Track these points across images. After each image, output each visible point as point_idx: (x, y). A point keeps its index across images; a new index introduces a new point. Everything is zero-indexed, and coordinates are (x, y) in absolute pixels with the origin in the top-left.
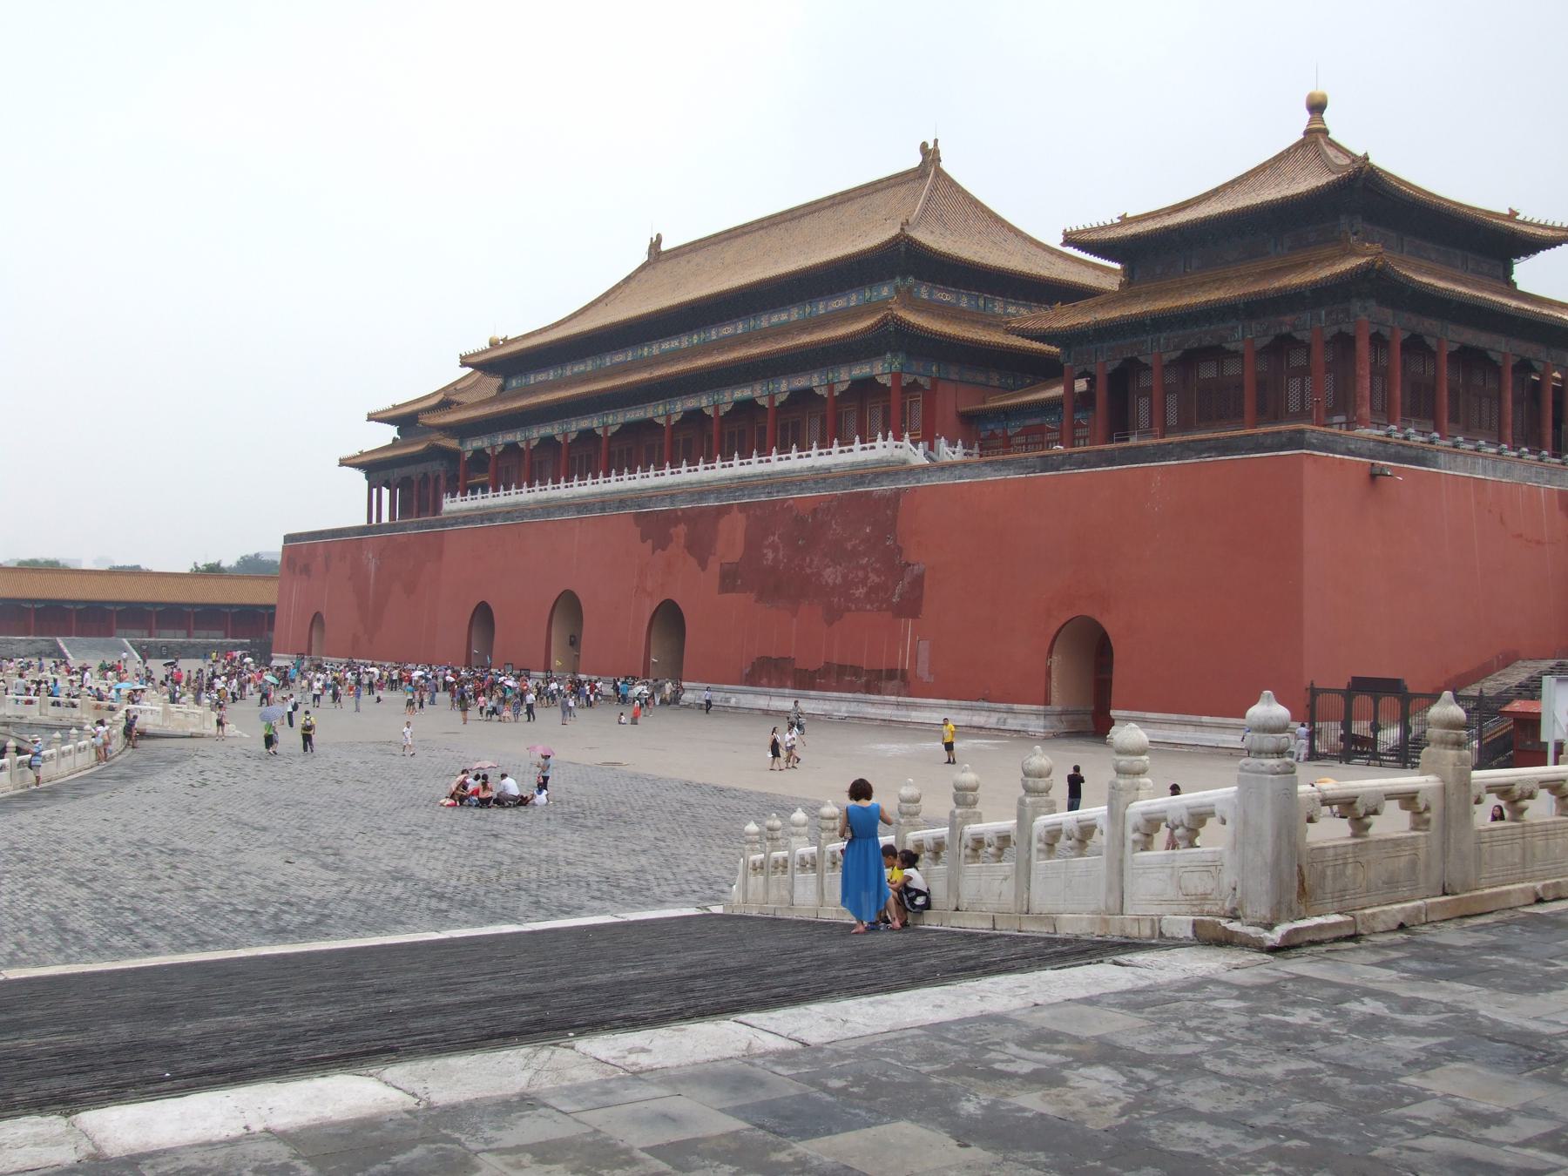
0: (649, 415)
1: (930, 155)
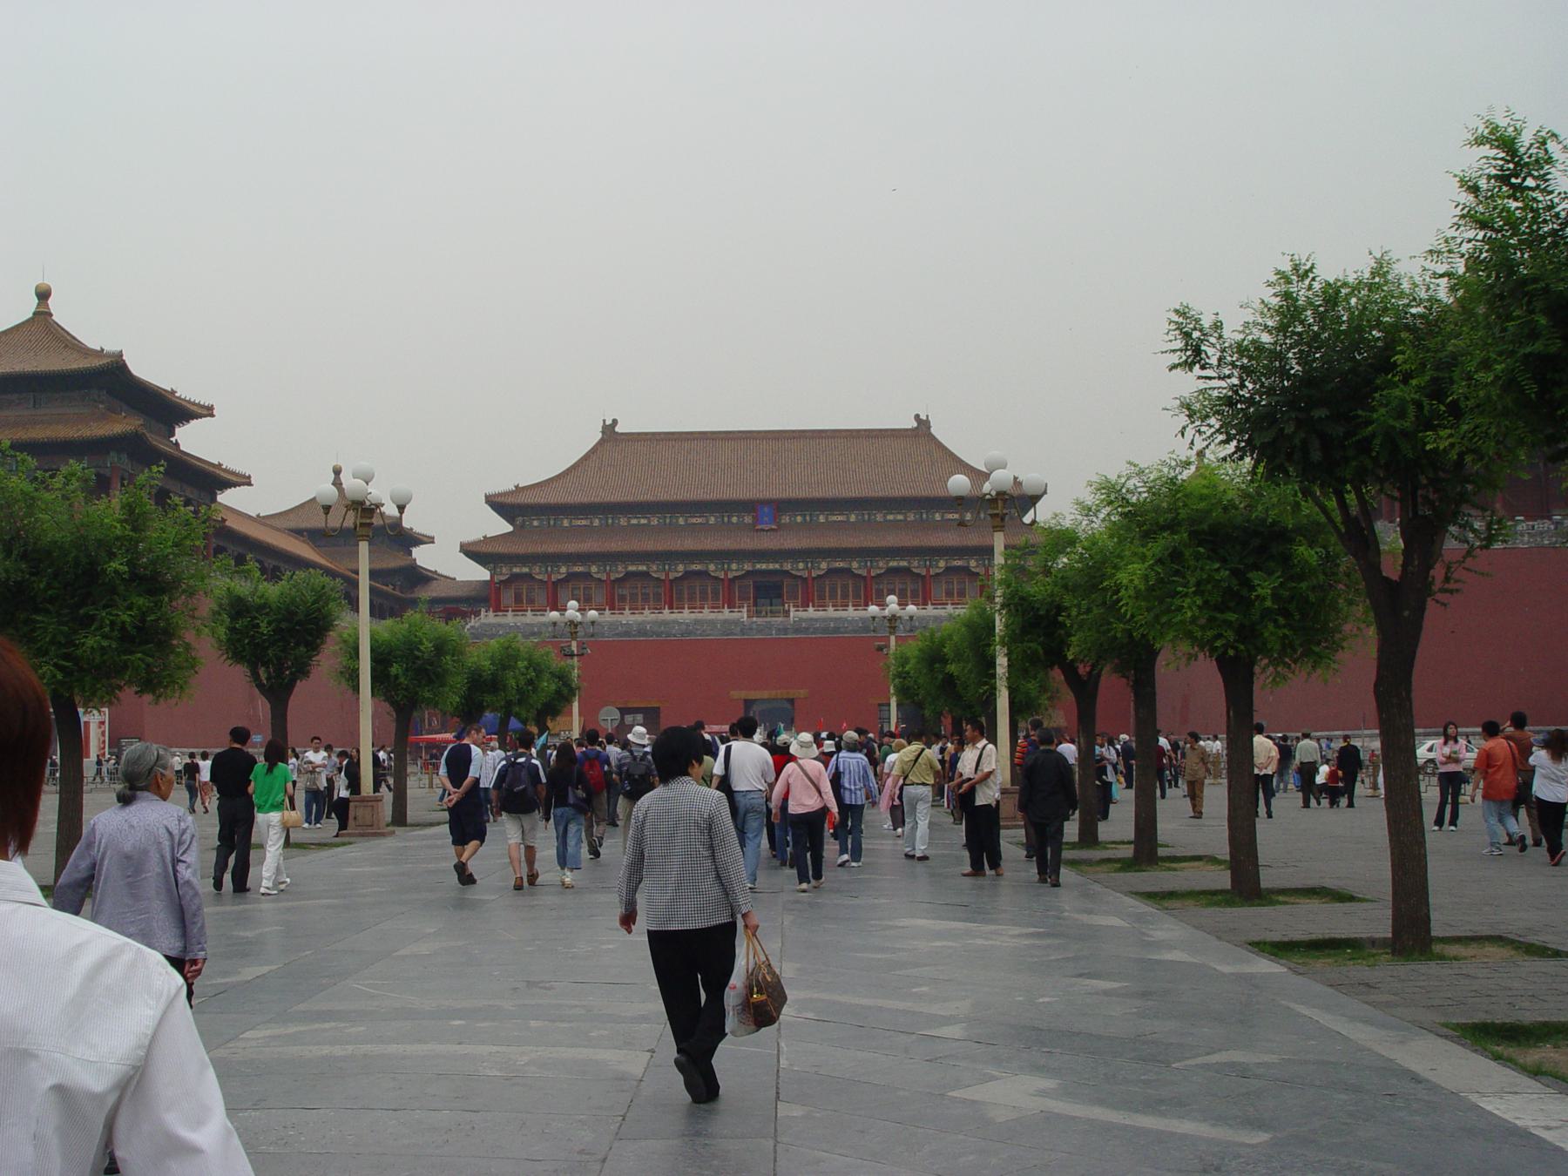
1: (923, 425)
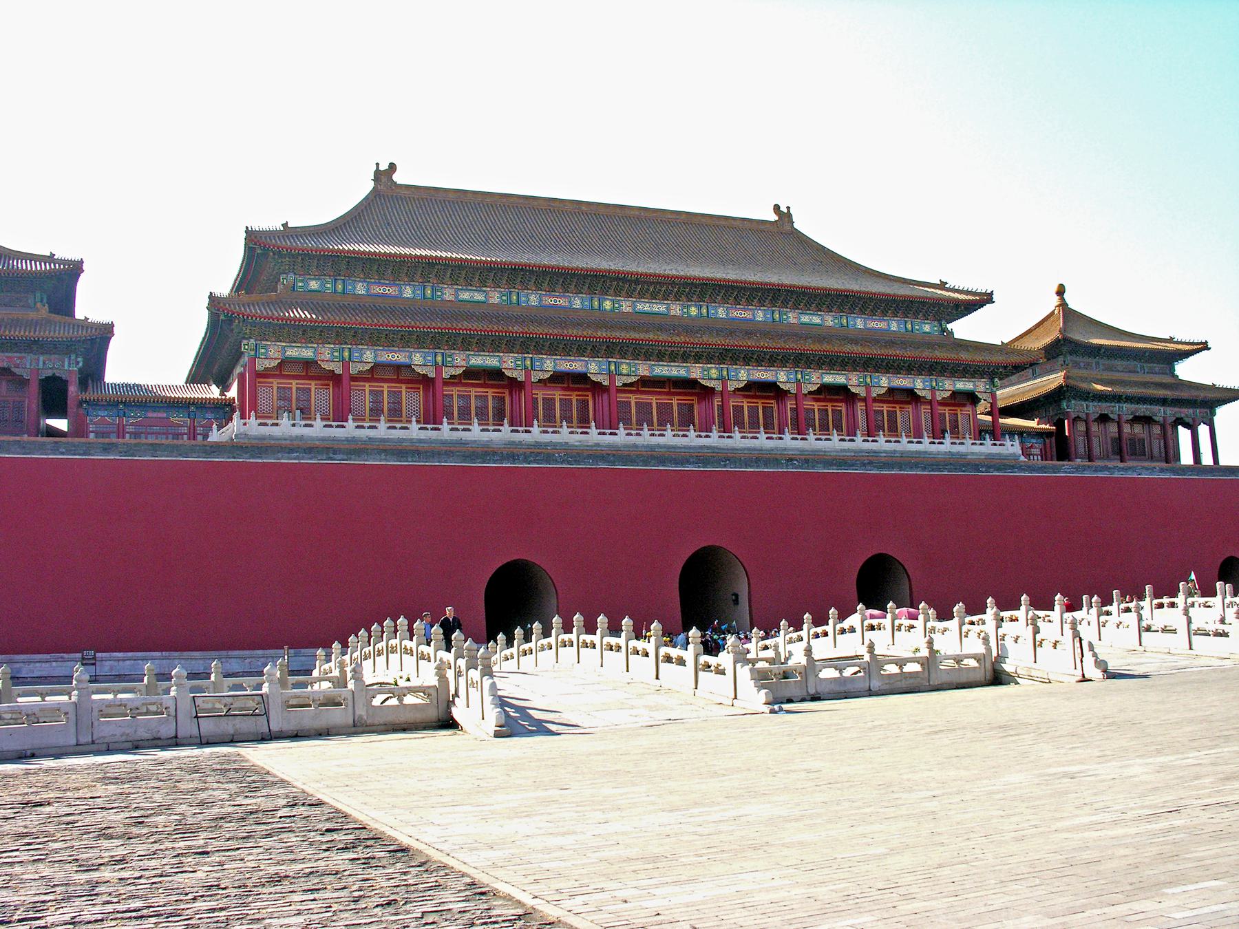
0: (693, 376)
1: (785, 217)
